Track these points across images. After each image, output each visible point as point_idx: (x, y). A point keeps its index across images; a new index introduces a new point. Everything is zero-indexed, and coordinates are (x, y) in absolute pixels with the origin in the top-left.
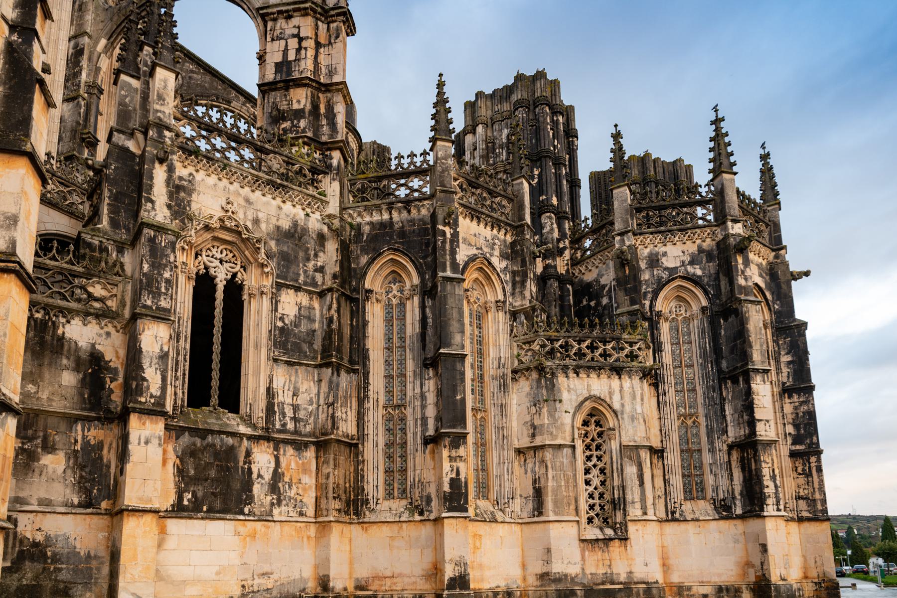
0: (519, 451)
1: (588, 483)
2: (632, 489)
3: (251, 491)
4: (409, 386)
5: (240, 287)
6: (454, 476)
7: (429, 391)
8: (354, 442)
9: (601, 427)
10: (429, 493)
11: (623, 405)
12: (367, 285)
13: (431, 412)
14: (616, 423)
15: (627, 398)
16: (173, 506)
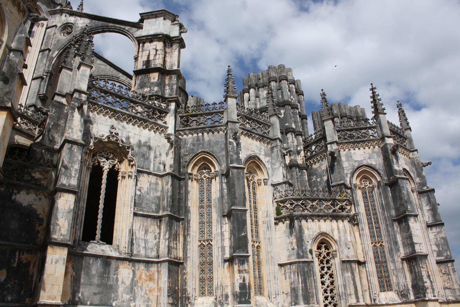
0: (281, 265)
1: (323, 283)
2: (349, 287)
3: (117, 292)
4: (214, 228)
5: (117, 172)
6: (241, 282)
7: (226, 231)
8: (181, 261)
9: (328, 250)
10: (227, 293)
11: (340, 237)
12: (189, 171)
13: (227, 243)
14: (337, 247)
15: (342, 233)
16: (69, 301)
